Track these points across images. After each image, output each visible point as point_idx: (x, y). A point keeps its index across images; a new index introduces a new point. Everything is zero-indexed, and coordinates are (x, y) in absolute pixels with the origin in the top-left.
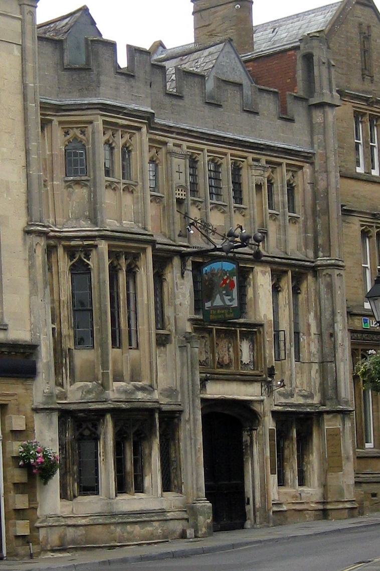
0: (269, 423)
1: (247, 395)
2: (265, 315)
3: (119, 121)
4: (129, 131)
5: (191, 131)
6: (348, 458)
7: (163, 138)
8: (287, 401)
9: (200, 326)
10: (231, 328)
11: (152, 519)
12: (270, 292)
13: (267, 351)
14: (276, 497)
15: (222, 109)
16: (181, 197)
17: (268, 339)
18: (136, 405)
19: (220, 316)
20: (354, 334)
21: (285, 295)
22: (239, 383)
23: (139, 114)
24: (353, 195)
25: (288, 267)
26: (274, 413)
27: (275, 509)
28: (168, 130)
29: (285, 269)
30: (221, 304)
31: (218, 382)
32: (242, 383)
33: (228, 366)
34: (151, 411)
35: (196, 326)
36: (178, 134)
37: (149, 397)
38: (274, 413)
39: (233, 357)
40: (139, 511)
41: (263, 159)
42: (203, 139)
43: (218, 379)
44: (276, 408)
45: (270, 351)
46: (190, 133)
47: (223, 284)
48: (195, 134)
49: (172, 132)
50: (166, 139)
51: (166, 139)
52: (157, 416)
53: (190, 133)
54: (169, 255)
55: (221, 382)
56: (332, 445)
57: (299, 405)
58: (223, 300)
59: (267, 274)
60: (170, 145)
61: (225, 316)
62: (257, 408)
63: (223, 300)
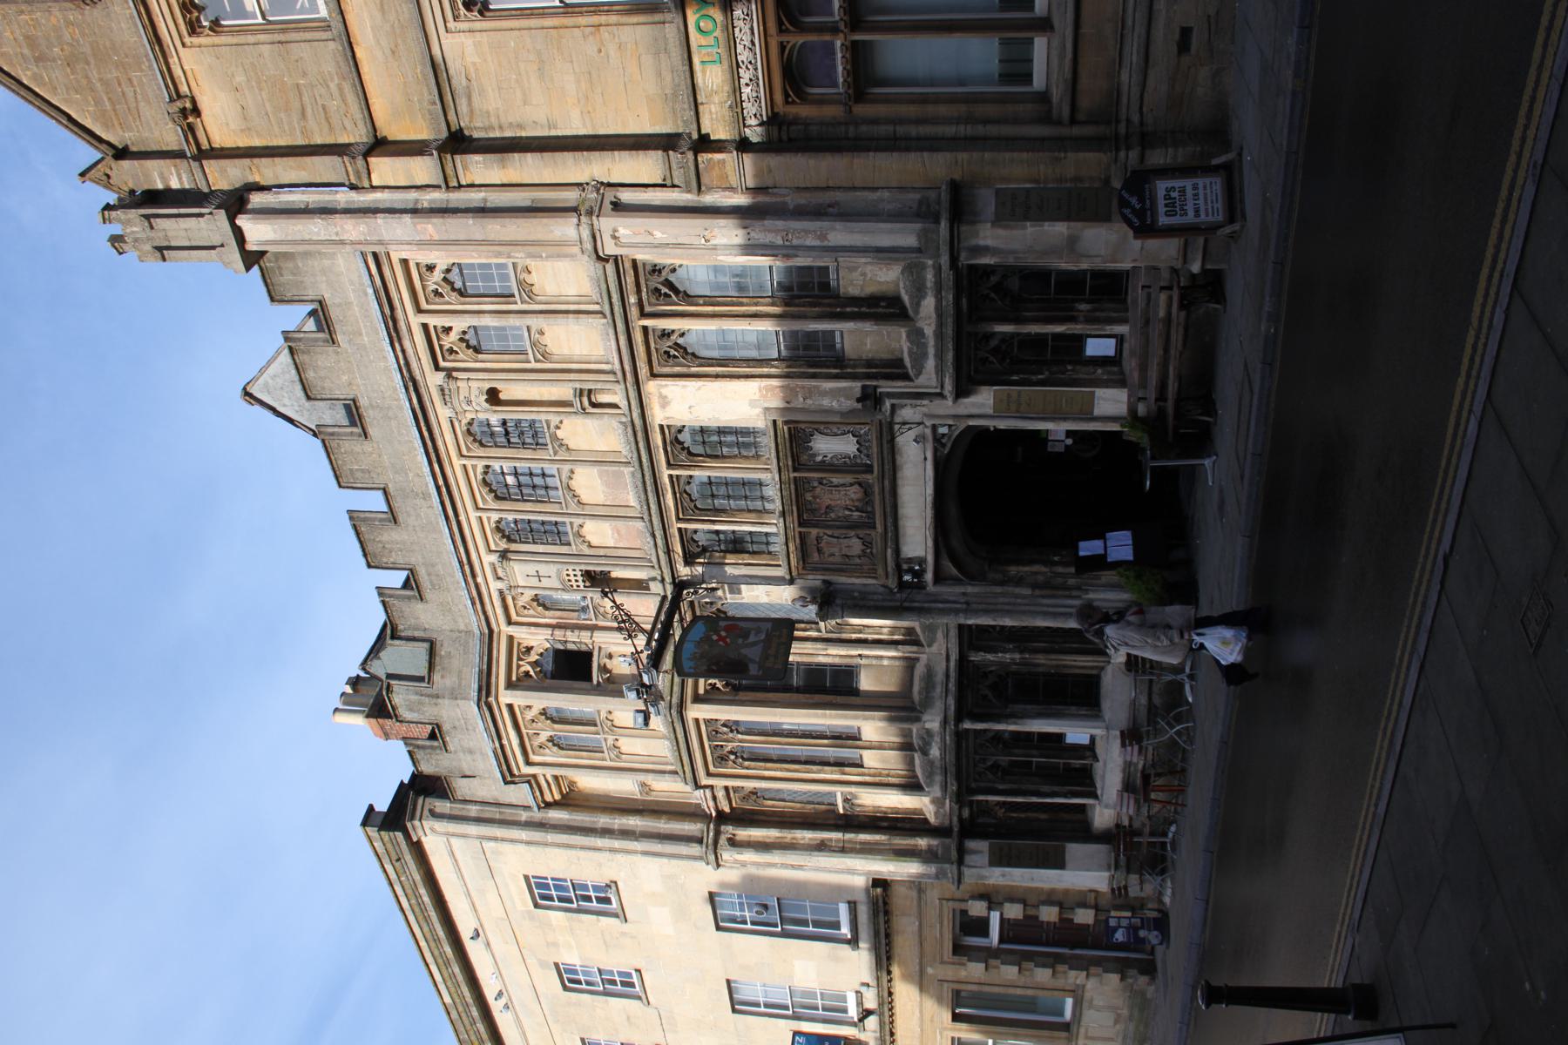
0: (983, 401)
2: (752, 403)
5: (461, 562)
8: (931, 351)
12: (699, 388)
13: (826, 402)
15: (390, 486)
16: (580, 579)
17: (801, 399)
18: (951, 758)
20: (744, 97)
21: (698, 330)
22: (900, 482)
24: (393, 52)
26: (961, 392)
28: (478, 599)
29: (638, 337)
32: (899, 475)
33: (866, 489)
34: (960, 736)
36: (474, 576)
37: (937, 739)
39: (849, 479)
44: (949, 387)
45: (824, 394)
47: (726, 643)
49: (477, 586)
52: (967, 725)
55: (901, 523)
57: (939, 309)
58: (754, 644)
59: (664, 391)
60: (495, 586)
63: (754, 644)
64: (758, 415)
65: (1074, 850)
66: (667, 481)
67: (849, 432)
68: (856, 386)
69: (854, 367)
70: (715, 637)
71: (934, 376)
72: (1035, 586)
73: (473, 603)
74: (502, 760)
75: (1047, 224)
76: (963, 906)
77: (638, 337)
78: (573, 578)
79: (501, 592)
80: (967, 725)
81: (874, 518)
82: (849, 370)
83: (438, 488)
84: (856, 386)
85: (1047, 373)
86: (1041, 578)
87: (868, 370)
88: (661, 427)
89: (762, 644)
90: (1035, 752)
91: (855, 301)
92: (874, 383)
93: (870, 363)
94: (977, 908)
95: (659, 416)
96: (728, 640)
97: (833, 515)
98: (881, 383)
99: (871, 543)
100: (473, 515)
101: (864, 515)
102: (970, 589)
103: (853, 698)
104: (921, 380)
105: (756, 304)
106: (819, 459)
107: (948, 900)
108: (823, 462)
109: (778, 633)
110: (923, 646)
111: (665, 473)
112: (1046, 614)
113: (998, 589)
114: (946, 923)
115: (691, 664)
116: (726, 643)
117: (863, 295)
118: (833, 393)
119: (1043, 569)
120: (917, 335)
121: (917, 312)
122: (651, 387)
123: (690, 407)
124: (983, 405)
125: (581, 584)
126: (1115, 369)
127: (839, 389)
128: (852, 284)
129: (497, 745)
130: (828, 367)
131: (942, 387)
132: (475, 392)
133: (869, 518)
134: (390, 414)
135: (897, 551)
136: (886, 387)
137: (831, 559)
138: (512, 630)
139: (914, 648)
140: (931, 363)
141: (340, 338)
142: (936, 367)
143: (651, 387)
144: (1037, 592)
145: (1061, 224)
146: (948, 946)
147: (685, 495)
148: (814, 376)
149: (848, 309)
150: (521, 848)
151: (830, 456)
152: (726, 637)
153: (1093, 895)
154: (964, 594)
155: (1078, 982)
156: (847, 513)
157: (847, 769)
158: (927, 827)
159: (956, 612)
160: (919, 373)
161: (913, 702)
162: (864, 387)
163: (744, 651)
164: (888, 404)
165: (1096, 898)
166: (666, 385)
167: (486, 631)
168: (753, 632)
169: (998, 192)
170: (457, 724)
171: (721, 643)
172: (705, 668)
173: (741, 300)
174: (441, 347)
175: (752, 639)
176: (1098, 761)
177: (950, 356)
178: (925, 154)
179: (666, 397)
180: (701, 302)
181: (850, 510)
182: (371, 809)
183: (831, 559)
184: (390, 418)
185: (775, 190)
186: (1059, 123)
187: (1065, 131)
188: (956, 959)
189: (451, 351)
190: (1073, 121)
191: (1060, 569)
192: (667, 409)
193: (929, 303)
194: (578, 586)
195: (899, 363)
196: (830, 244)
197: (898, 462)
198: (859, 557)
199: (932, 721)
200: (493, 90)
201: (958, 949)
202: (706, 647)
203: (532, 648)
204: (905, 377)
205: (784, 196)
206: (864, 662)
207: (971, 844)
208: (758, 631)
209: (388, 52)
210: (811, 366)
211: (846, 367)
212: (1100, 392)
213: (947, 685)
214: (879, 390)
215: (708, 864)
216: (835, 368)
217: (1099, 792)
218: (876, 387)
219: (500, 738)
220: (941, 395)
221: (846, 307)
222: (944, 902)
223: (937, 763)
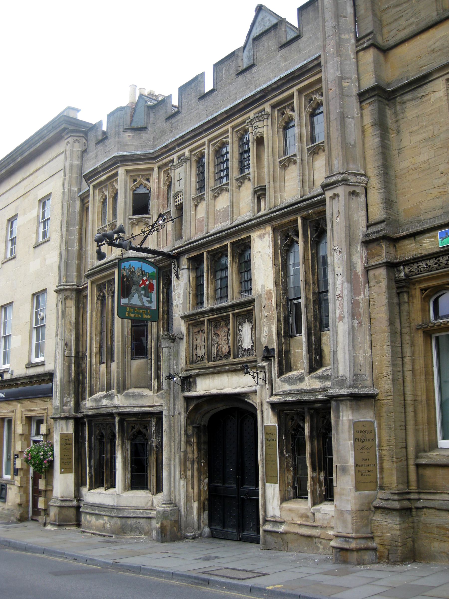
1: (240, 387)
2: (263, 286)
3: (102, 179)
4: (113, 180)
6: (344, 470)
7: (168, 158)
9: (194, 321)
10: (222, 315)
11: (102, 513)
12: (269, 256)
14: (277, 513)
15: (216, 92)
16: (179, 203)
17: (266, 315)
19: (137, 316)
20: (420, 264)
22: (230, 374)
23: (110, 164)
24: (433, 50)
25: (296, 214)
26: (273, 405)
27: (268, 527)
29: (292, 218)
30: (139, 303)
31: (207, 377)
32: (233, 373)
34: (111, 415)
35: (190, 322)
36: (179, 145)
37: (110, 403)
38: (273, 405)
40: (99, 504)
41: (267, 107)
42: (201, 133)
43: (208, 374)
44: (275, 399)
46: (184, 139)
47: (142, 284)
48: (189, 136)
49: (174, 148)
50: (171, 158)
51: (171, 158)
52: (117, 419)
53: (184, 139)
54: (168, 262)
55: (211, 376)
56: (362, 448)
58: (141, 300)
59: (267, 236)
61: (142, 316)
62: (255, 401)
64: (258, 291)
65: (71, 478)
66: (225, 244)
67: (253, 343)
68: (274, 346)
69: (286, 344)
70: (145, 278)
71: (281, 390)
72: (185, 452)
73: (165, 147)
74: (93, 173)
75: (353, 453)
76: (45, 421)
77: (292, 218)
78: (179, 199)
79: (172, 161)
80: (117, 419)
81: (214, 361)
82: (283, 341)
83: (215, 118)
84: (274, 346)
85: (287, 455)
86: (190, 455)
87: (283, 351)
88: (250, 236)
89: (141, 304)
90: (109, 455)
91: (319, 341)
92: (276, 357)
93: (288, 352)
94: (43, 428)
95: (255, 235)
96: (143, 286)
97: (214, 338)
98: (276, 360)
99: (202, 360)
100: (206, 140)
101: (215, 355)
102: (182, 416)
103: (130, 356)
104: (278, 381)
105: (314, 283)
106: (240, 327)
107: (47, 413)
108: (239, 330)
109: (149, 312)
110: (157, 392)
111: (228, 242)
112: (169, 459)
113: (183, 432)
114: (38, 412)
115: (127, 267)
116: (142, 284)
117: (322, 345)
118: (270, 332)
119: (196, 455)
120: (301, 379)
121: (312, 378)
122: (269, 229)
123: (259, 252)
124: (268, 419)
125: (177, 204)
126: (292, 495)
127: (272, 335)
128: (327, 339)
129: (99, 170)
130: (284, 328)
131: (276, 395)
132: (261, 130)
133: (214, 358)
134: (249, 86)
135: (198, 375)
136: (275, 363)
137: (195, 339)
138: (156, 169)
139: (156, 388)
140: (287, 387)
141: (283, 51)
142: (285, 391)
143: (269, 229)
144: (182, 454)
145: (353, 461)
146: (29, 414)
147: (220, 255)
148: (279, 320)
149: (313, 337)
150: (61, 189)
151: (241, 333)
152: (145, 284)
153: (51, 488)
154: (179, 413)
155: (16, 482)
156: (216, 345)
157: (98, 356)
158: (80, 400)
159: (169, 410)
160: (283, 381)
161: (128, 389)
162: (273, 350)
163: (136, 295)
164: (264, 364)
165: (50, 490)
166: (269, 237)
167: (154, 156)
168: (149, 299)
169: (373, 423)
170: (108, 147)
171: (141, 282)
172: (125, 274)
173: (316, 274)
174: (284, 108)
175: (145, 299)
176: (106, 490)
177: (290, 399)
178: (391, 376)
179: (264, 237)
180: (313, 251)
181: (217, 347)
182: (78, 110)
183: (195, 339)
184: (246, 86)
185: (367, 288)
186: (417, 457)
187: (411, 462)
188: (24, 418)
189: (283, 114)
190: (418, 466)
191: (196, 466)
192: (259, 239)
193: (317, 384)
194: (176, 202)
195: (289, 369)
196: (337, 323)
197: (238, 373)
198: (196, 355)
199: (118, 400)
200: (417, 113)
201: (29, 419)
202: (139, 274)
203: (149, 182)
204: (281, 373)
205: (364, 294)
206: (149, 361)
207: (71, 424)
208: (150, 302)
209: (433, 47)
210: (285, 318)
211: (285, 339)
212: (277, 486)
213: (137, 407)
214: (272, 359)
215: (57, 287)
216: (284, 332)
217: (92, 491)
218: (274, 357)
219: (104, 170)
220: (272, 395)
221: (315, 336)
222: (46, 411)
223: (100, 404)
